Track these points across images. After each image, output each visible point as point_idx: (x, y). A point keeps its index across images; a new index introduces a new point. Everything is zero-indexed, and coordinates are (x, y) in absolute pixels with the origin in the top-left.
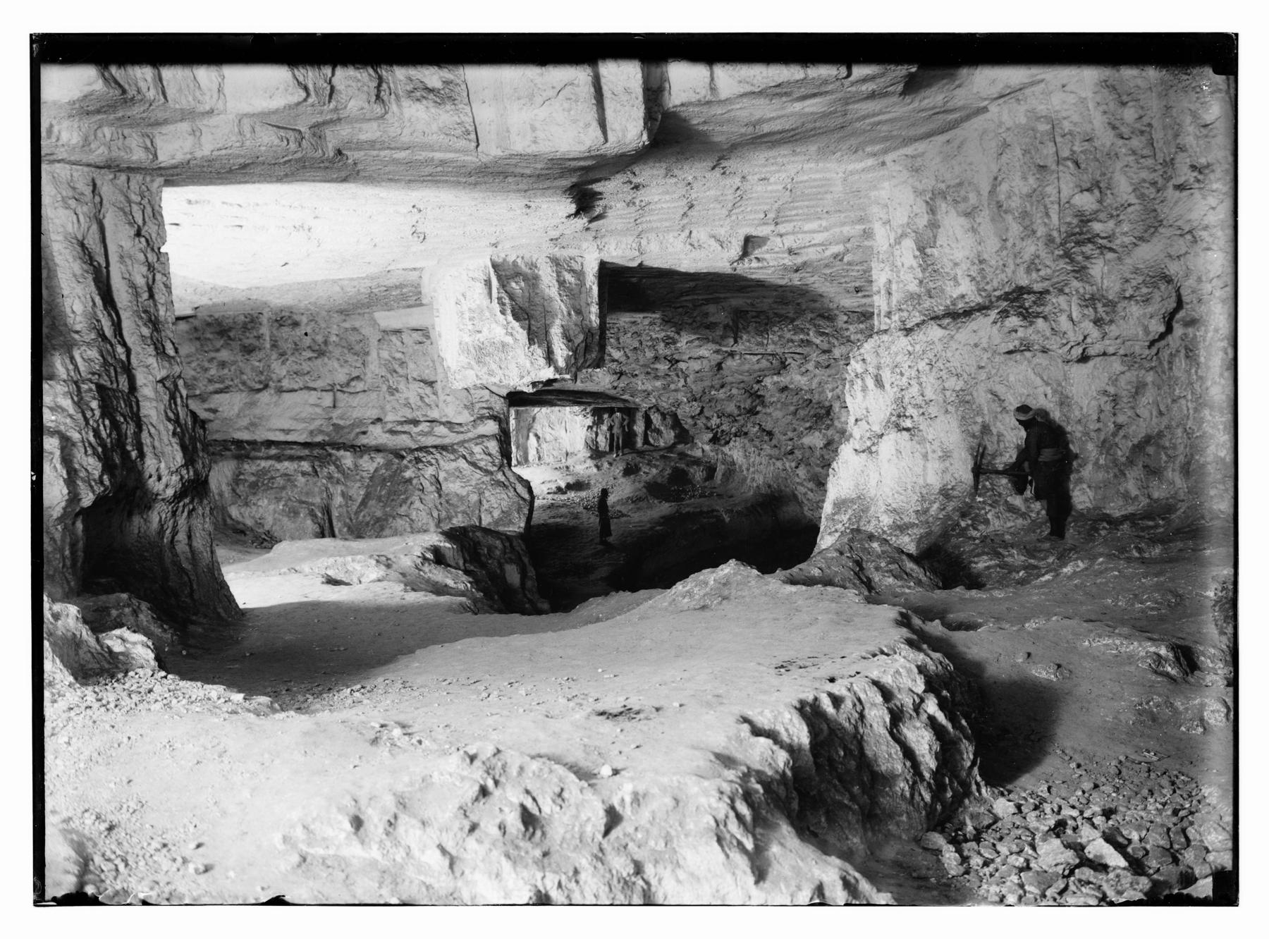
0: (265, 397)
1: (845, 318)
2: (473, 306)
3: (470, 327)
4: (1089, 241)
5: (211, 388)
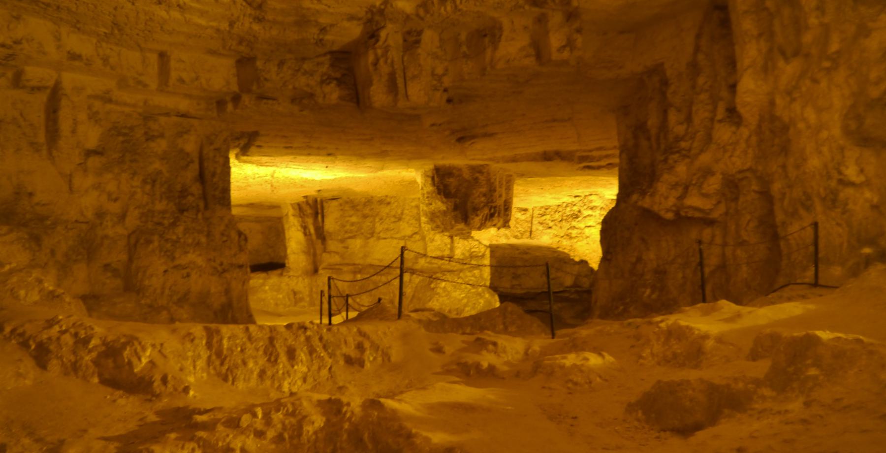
0: (372, 240)
4: (678, 152)
5: (347, 235)
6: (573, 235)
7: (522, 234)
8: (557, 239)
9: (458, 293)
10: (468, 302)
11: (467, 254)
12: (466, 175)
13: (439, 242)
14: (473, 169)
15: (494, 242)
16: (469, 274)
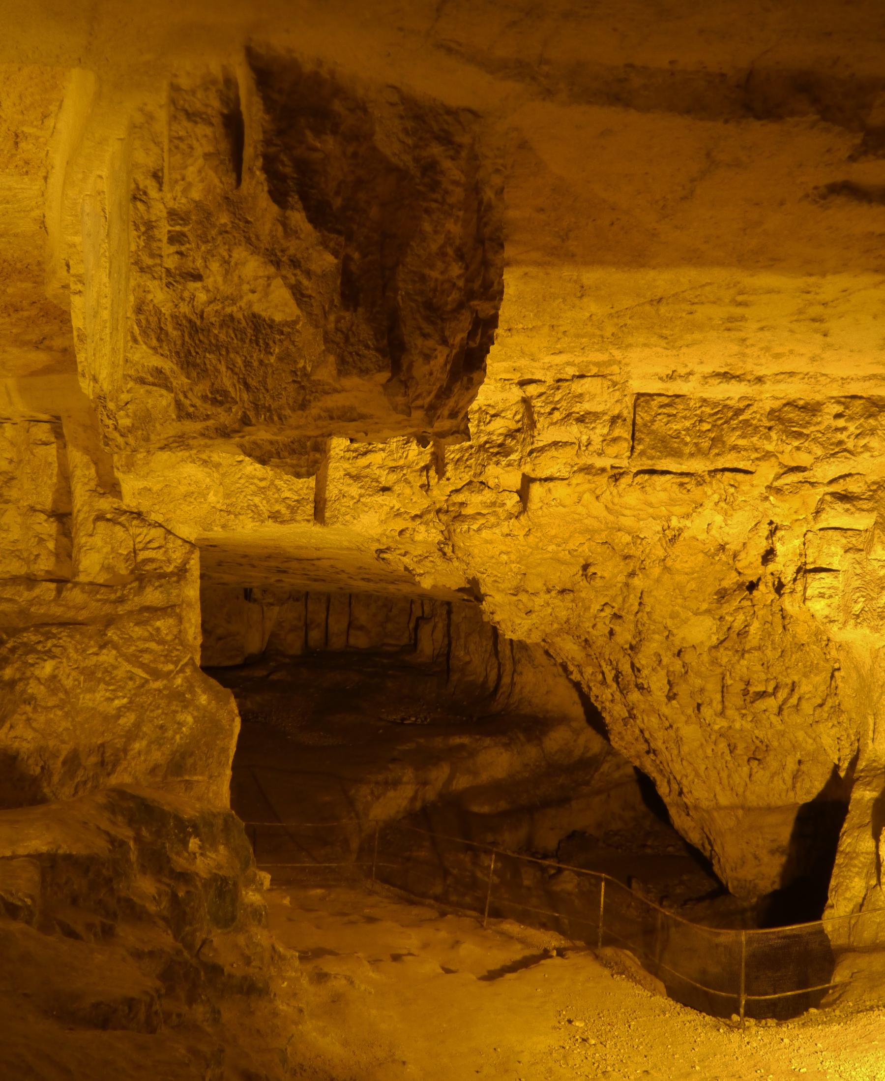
1: (839, 409)
2: (182, 204)
3: (171, 262)
6: (469, 511)
7: (293, 510)
8: (399, 524)
9: (101, 693)
10: (137, 725)
11: (123, 569)
12: (390, 141)
13: (15, 533)
14: (429, 122)
15: (217, 533)
16: (138, 631)
